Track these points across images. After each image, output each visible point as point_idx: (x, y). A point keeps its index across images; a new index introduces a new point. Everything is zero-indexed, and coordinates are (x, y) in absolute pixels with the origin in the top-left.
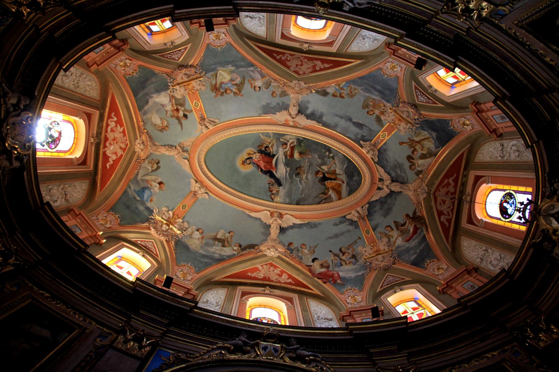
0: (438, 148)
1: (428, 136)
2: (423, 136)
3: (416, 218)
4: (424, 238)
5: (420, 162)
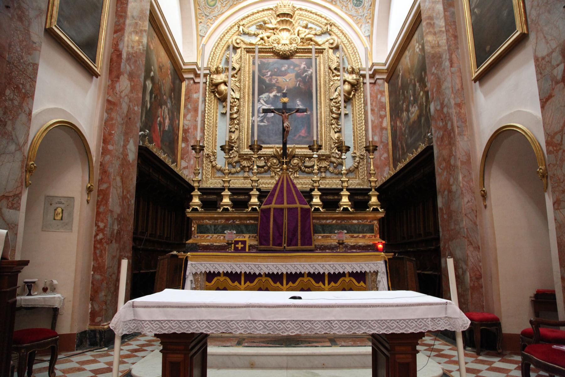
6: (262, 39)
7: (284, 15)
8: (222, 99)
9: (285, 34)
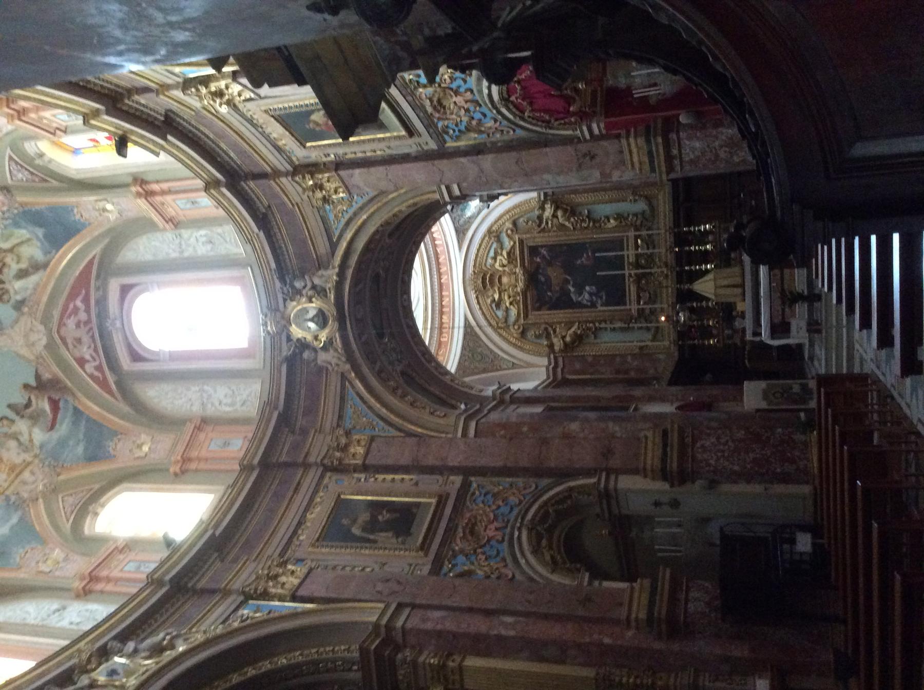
0: (50, 253)
1: (28, 236)
2: (18, 238)
3: (42, 386)
4: (77, 412)
5: (18, 284)
6: (511, 303)
7: (484, 282)
8: (579, 339)
9: (505, 280)
